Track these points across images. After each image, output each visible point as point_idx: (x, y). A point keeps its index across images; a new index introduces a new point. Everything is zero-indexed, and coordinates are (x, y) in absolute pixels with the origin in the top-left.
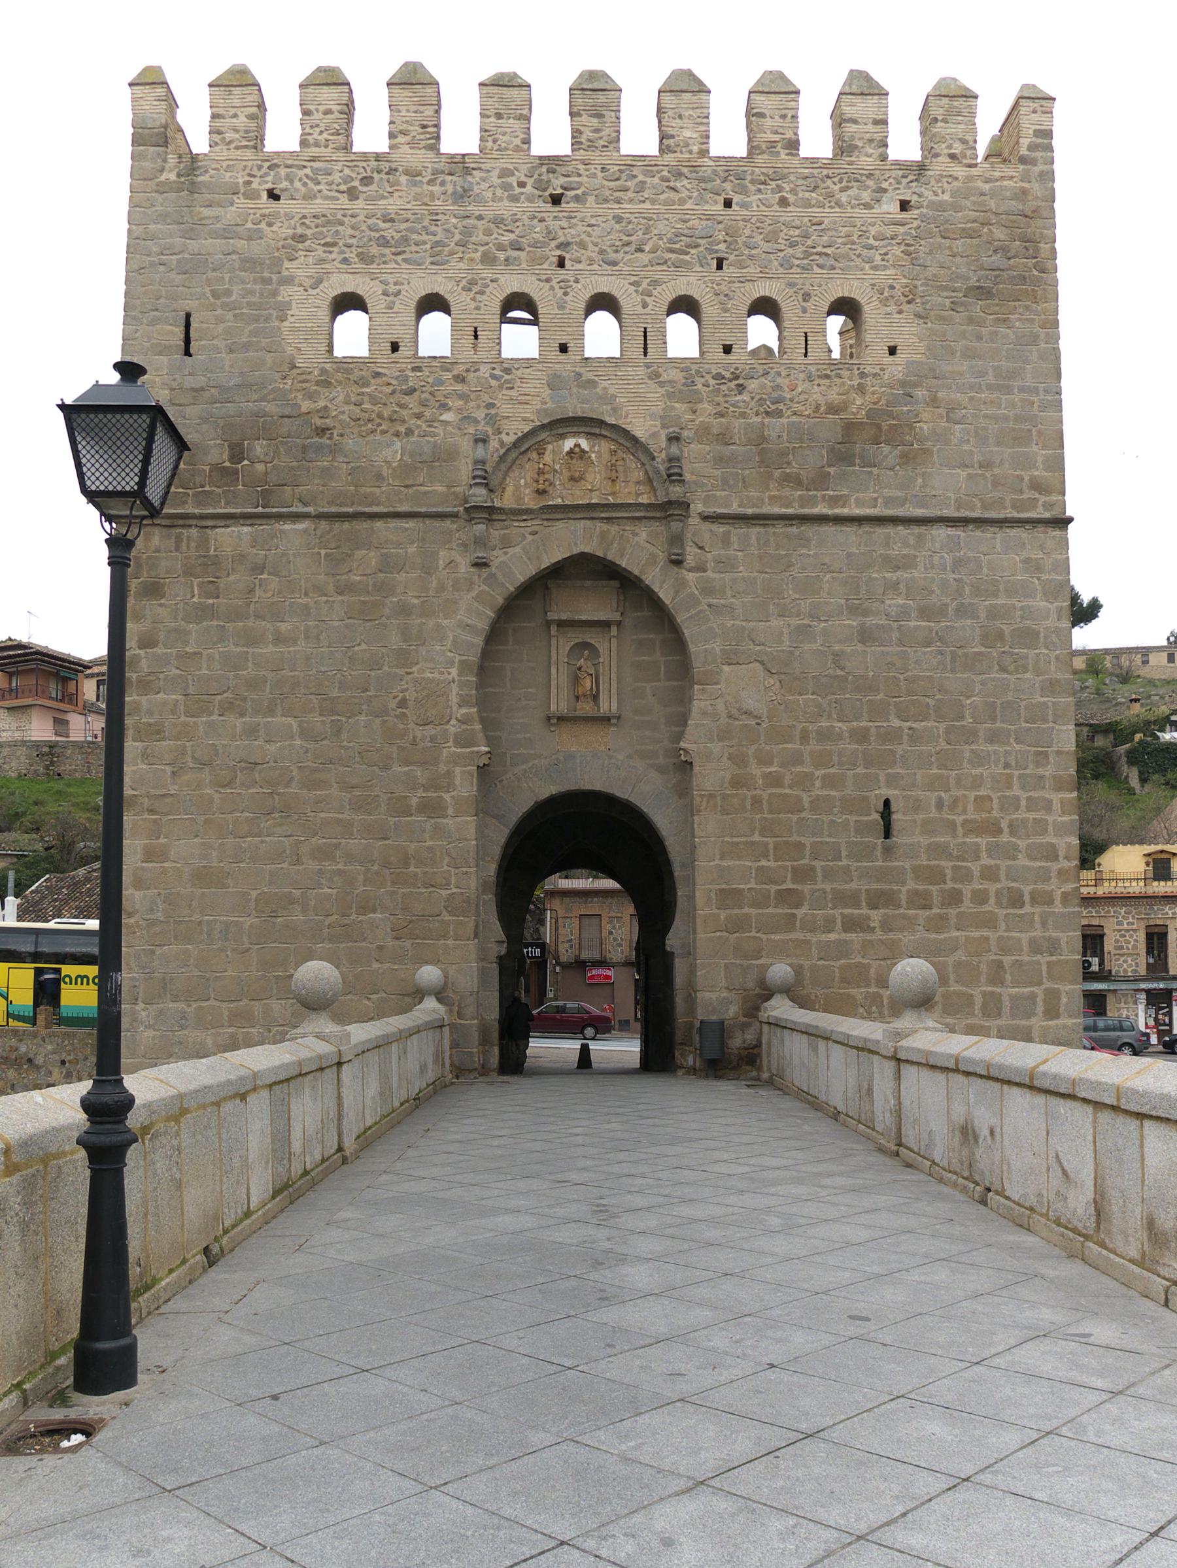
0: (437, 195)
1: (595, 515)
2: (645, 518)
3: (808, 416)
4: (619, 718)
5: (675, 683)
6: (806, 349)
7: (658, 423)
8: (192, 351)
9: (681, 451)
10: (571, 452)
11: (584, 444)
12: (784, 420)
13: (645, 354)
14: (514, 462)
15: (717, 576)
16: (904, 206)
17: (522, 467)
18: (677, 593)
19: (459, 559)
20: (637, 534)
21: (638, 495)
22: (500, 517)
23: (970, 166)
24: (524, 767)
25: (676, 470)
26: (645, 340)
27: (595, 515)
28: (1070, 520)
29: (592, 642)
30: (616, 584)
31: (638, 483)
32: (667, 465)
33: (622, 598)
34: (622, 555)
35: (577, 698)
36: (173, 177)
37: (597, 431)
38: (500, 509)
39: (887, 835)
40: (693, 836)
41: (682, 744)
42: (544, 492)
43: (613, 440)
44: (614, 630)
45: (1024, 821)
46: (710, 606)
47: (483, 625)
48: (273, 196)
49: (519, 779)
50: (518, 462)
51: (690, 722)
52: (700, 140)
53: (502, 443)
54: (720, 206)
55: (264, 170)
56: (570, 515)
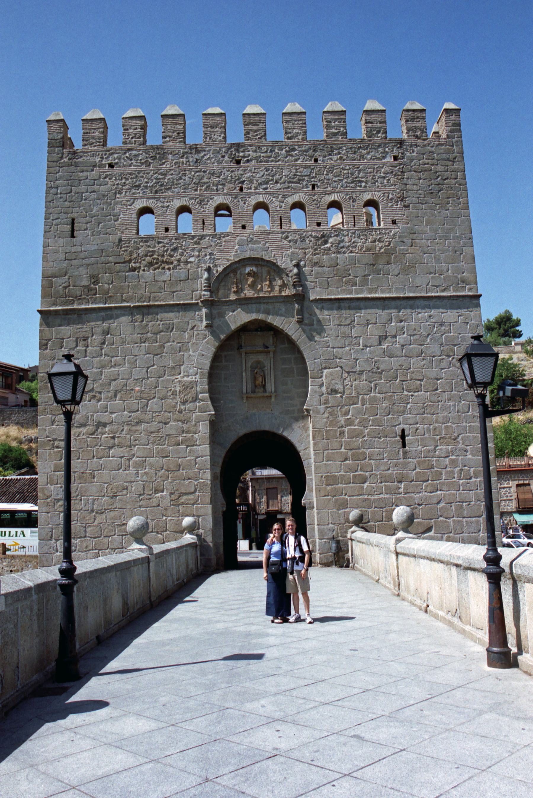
0: (185, 163)
3: (358, 253)
6: (355, 223)
8: (75, 235)
11: (254, 269)
12: (346, 255)
13: (281, 228)
16: (395, 158)
20: (281, 309)
23: (424, 140)
26: (281, 222)
28: (480, 296)
30: (272, 333)
33: (275, 339)
36: (66, 160)
39: (404, 446)
45: (468, 437)
47: (210, 355)
48: (111, 166)
52: (302, 134)
54: (313, 162)
55: (106, 156)
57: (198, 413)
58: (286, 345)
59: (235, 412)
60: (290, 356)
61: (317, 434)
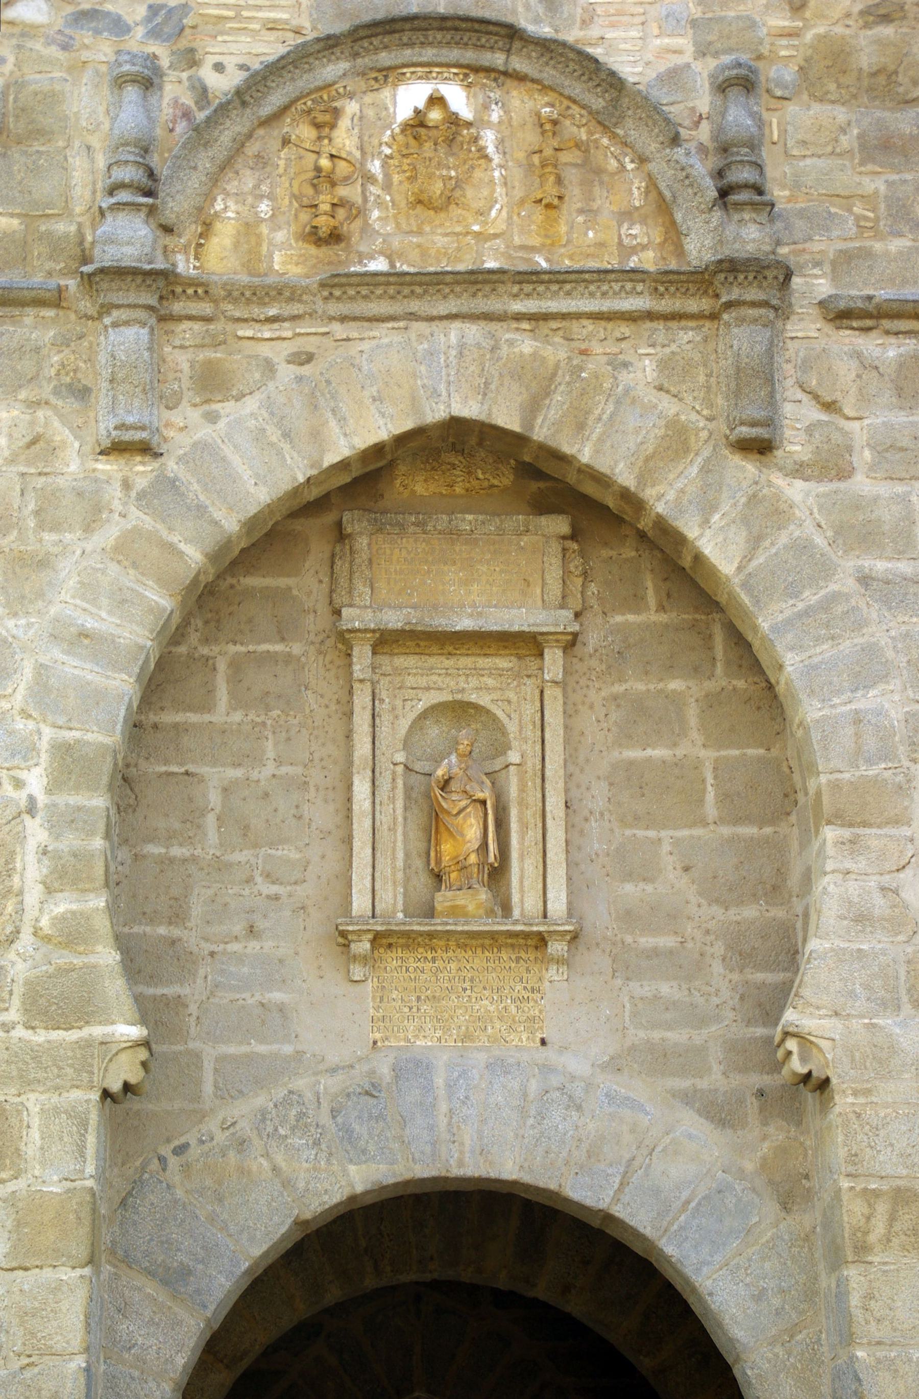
1: (494, 305)
2: (650, 316)
4: (574, 937)
5: (749, 831)
7: (685, 42)
9: (761, 124)
10: (418, 122)
14: (239, 146)
15: (884, 489)
17: (261, 161)
18: (755, 542)
19: (61, 432)
21: (634, 250)
22: (195, 308)
24: (260, 1100)
25: (745, 175)
27: (494, 305)
29: (484, 700)
30: (560, 525)
31: (627, 215)
32: (714, 162)
33: (576, 564)
34: (581, 426)
35: (438, 877)
37: (498, 59)
38: (194, 283)
40: (847, 1338)
41: (789, 1016)
42: (335, 237)
43: (545, 88)
44: (554, 660)
46: (865, 580)
49: (242, 1144)
50: (252, 148)
51: (814, 944)
53: (202, 93)
56: (415, 306)
57: (20, 1032)
58: (654, 617)
59: (288, 1049)
60: (675, 685)
61: (879, 1227)
